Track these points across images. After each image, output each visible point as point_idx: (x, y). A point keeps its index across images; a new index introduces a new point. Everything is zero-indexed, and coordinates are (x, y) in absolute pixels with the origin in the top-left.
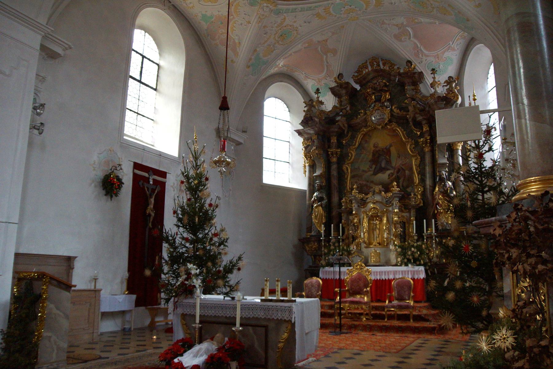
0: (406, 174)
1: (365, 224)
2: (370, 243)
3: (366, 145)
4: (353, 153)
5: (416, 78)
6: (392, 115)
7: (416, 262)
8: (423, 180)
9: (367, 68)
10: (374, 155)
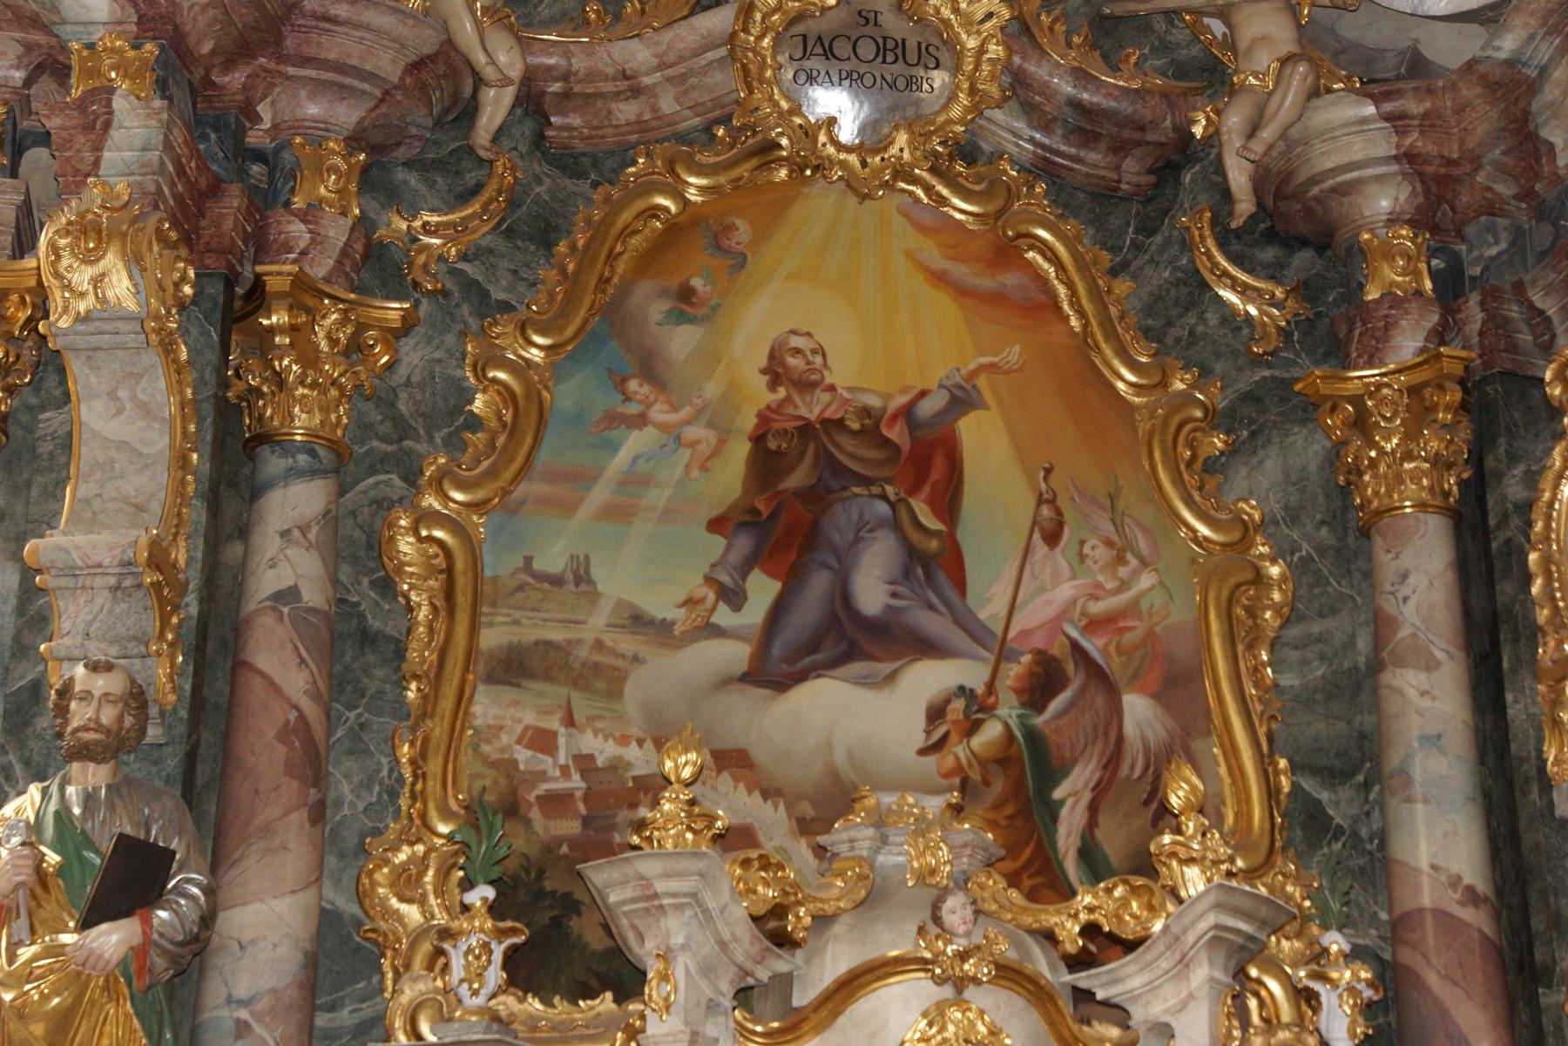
0: (1129, 728)
3: (681, 342)
10: (766, 461)
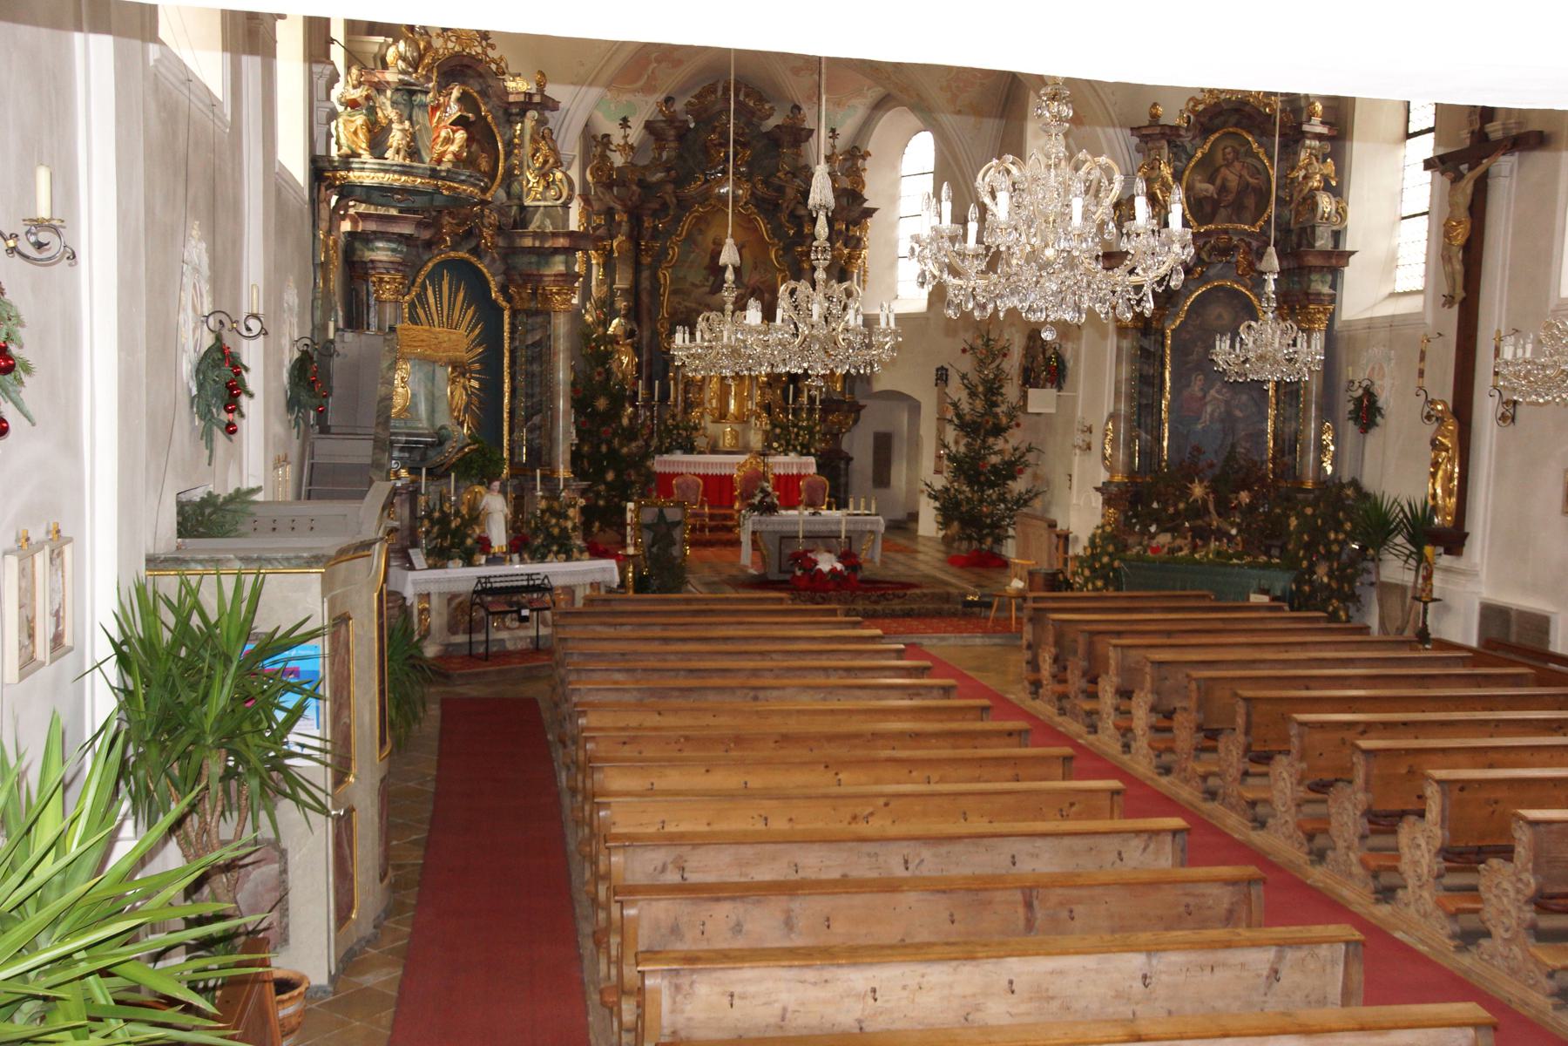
3: (700, 238)
4: (674, 252)
6: (753, 194)
7: (805, 451)
9: (715, 92)
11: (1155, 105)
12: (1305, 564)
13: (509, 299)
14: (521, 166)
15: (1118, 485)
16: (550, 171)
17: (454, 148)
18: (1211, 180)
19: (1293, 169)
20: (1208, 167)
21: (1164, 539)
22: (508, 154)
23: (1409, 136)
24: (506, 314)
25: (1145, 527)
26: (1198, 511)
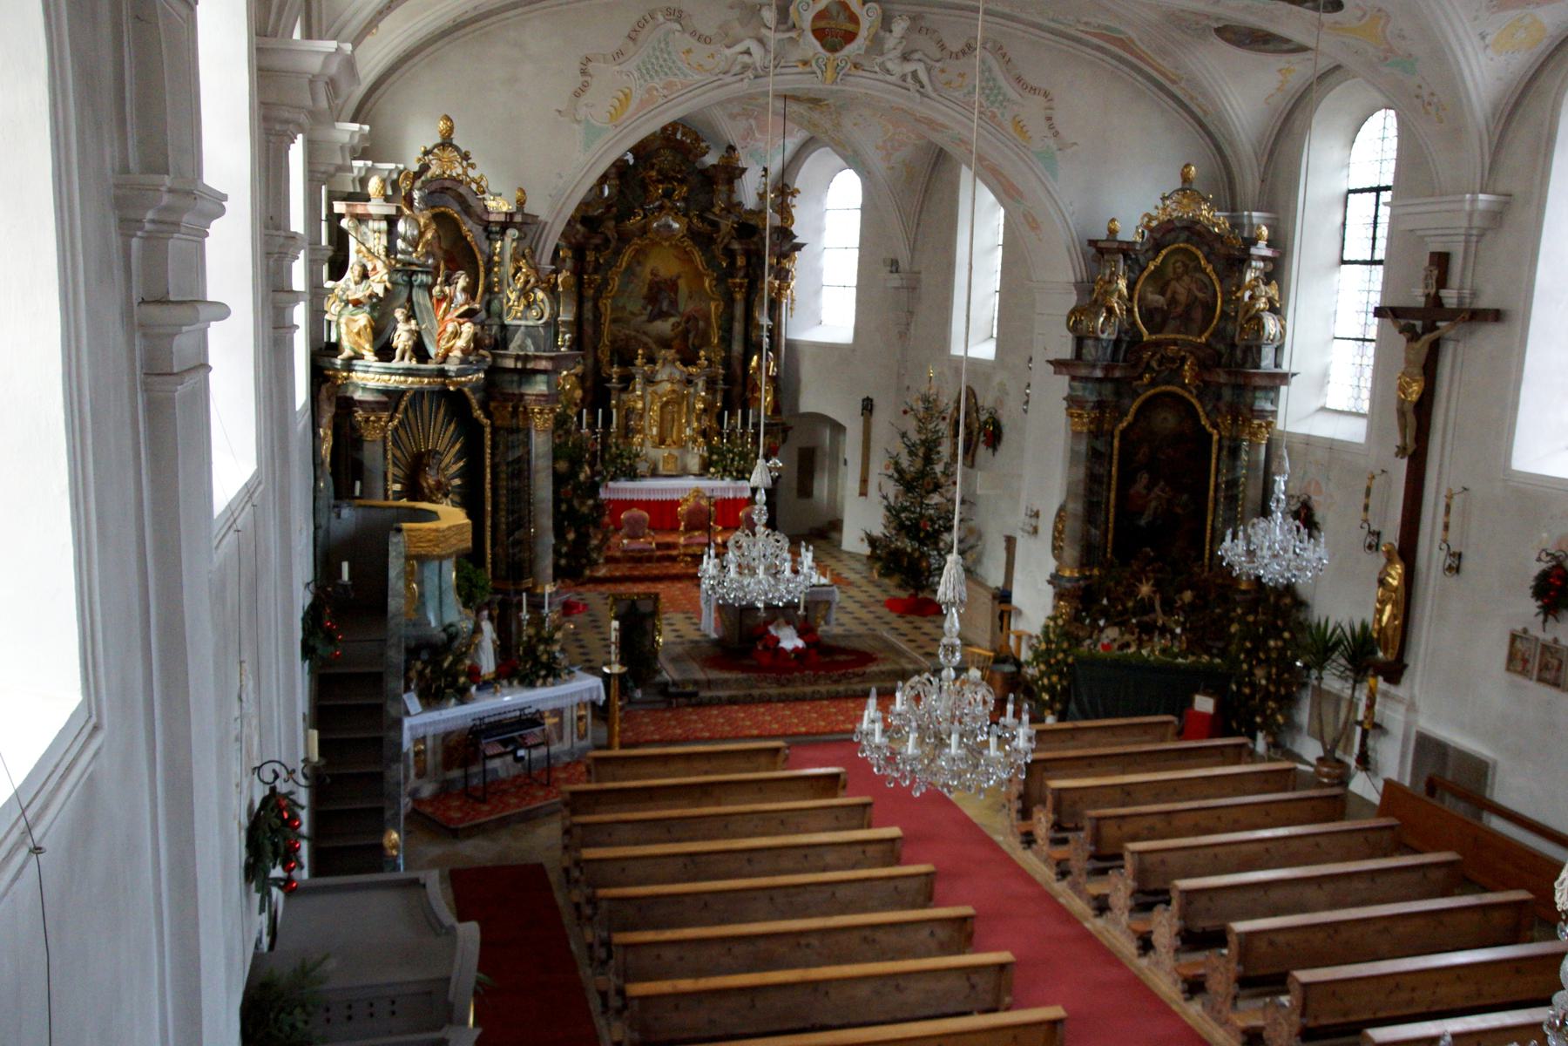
1: (654, 413)
2: (662, 442)
3: (638, 269)
4: (616, 283)
5: (731, 172)
6: (689, 229)
8: (726, 341)
10: (650, 288)
11: (1113, 220)
12: (1245, 666)
13: (489, 415)
14: (500, 282)
15: (1070, 580)
16: (532, 290)
17: (461, 343)
18: (1162, 293)
19: (1239, 288)
20: (1160, 280)
21: (1112, 633)
22: (489, 272)
23: (1343, 262)
24: (488, 430)
25: (1095, 621)
26: (1145, 607)
